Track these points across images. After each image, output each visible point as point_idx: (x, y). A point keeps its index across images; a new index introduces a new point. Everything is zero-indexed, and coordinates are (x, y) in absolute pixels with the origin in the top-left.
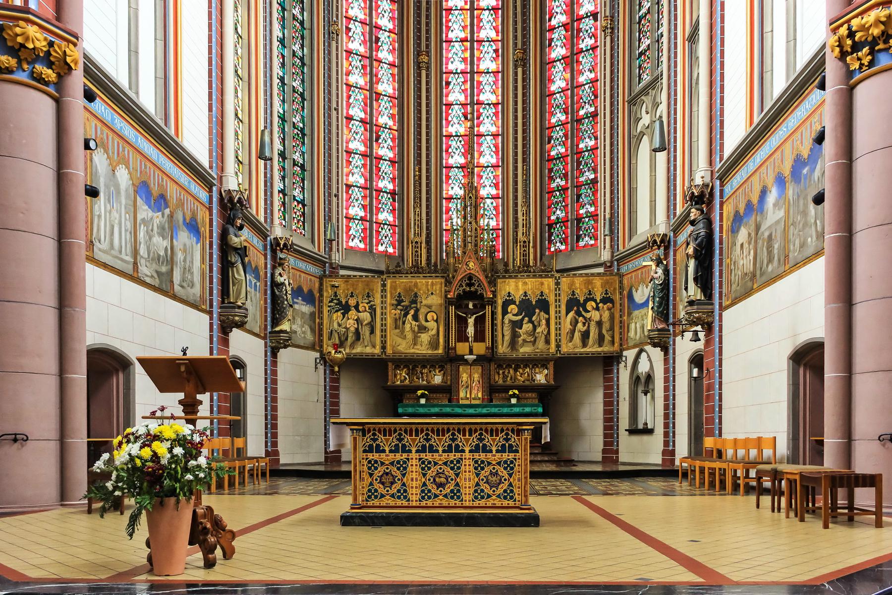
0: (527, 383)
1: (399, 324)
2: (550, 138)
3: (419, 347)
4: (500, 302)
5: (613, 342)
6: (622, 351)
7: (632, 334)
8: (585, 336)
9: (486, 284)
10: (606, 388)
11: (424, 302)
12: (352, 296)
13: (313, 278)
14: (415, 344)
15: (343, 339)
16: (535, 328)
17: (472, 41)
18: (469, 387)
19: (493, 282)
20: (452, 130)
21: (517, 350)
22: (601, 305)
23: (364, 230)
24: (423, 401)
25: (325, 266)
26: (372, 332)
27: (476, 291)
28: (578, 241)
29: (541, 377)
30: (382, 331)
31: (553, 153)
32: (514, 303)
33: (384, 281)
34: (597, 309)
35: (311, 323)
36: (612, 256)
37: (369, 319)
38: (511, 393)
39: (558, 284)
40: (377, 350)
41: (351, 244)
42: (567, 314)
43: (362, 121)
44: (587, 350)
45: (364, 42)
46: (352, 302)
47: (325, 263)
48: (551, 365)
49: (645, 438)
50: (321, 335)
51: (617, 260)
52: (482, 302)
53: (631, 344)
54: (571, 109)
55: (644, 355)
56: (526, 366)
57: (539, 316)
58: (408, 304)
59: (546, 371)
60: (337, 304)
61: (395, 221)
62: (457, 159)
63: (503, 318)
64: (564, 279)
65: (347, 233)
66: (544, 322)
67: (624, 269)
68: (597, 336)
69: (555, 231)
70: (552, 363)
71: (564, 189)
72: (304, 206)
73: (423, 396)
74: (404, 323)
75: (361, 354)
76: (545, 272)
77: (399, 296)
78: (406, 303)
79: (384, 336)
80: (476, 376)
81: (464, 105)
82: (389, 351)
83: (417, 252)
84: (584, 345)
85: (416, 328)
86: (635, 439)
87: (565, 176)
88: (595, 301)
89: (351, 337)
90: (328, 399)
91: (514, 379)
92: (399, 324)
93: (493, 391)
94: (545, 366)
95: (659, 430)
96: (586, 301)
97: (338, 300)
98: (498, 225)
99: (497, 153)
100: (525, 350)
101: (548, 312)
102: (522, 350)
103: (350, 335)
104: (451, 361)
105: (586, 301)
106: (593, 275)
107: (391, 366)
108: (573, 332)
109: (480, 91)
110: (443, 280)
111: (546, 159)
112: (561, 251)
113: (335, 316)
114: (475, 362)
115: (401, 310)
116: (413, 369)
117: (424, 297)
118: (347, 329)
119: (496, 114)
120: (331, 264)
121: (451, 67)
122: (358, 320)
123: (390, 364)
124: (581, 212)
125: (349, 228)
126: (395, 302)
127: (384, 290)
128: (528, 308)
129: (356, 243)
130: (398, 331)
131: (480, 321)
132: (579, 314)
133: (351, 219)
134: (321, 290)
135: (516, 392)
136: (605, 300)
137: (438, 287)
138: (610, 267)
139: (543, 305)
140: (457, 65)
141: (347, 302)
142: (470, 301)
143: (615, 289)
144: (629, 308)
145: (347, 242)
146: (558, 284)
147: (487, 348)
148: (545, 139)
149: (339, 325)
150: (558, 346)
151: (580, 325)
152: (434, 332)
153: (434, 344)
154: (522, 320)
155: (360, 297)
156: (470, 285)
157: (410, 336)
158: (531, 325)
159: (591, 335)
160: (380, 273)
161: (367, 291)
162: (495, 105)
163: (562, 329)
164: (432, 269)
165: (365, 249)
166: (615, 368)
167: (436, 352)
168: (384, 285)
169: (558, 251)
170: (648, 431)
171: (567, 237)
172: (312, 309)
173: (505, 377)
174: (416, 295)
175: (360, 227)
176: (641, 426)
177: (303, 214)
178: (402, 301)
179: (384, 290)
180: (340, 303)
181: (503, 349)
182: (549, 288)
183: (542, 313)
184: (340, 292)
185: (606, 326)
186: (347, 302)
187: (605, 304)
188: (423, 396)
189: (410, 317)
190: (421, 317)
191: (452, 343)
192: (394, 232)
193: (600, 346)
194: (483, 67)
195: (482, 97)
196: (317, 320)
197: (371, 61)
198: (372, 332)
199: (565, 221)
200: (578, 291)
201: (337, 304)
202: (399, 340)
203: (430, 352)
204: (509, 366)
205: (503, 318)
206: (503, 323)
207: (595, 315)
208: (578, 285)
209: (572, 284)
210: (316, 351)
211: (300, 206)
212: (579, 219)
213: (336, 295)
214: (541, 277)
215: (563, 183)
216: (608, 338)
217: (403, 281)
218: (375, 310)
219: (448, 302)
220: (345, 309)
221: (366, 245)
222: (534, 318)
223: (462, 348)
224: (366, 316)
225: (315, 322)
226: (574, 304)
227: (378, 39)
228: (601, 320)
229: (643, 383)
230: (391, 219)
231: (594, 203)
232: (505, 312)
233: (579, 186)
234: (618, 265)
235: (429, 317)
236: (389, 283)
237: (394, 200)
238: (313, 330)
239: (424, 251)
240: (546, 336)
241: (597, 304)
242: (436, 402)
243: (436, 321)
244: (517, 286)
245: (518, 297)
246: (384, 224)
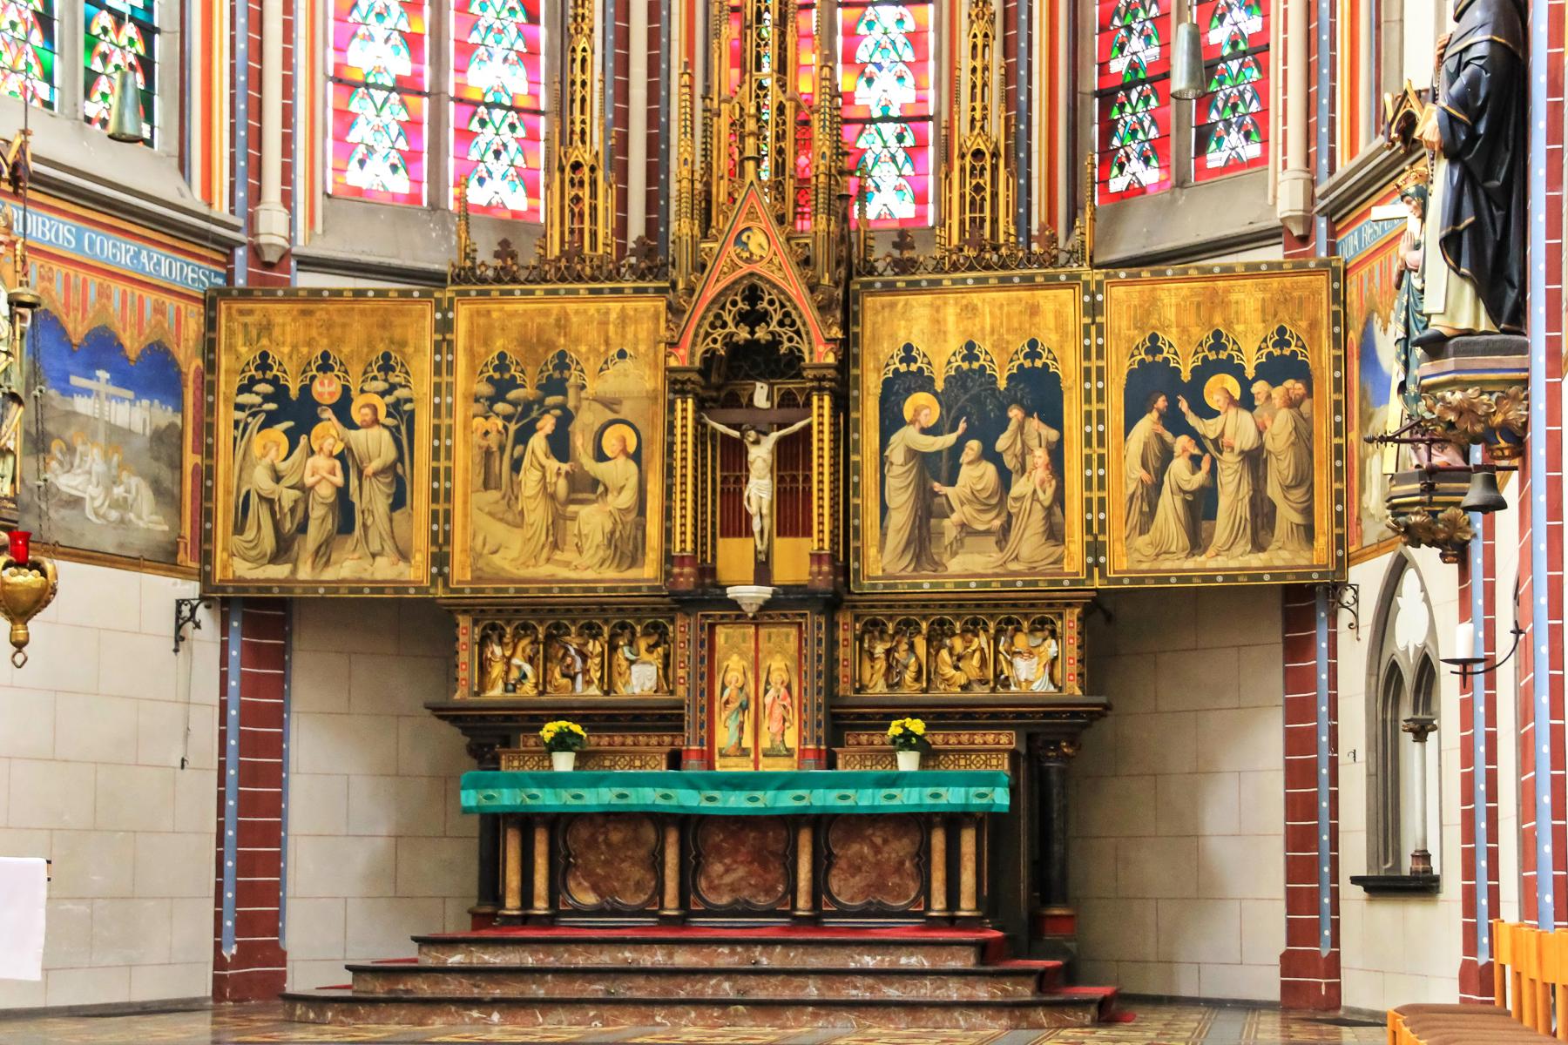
0: (980, 692)
1: (498, 469)
3: (568, 555)
5: (1308, 532)
6: (1343, 564)
8: (1201, 506)
10: (1298, 711)
11: (594, 386)
12: (325, 367)
13: (171, 302)
14: (555, 546)
15: (288, 526)
16: (1005, 478)
21: (937, 565)
22: (1259, 388)
23: (411, 127)
24: (564, 762)
25: (230, 258)
26: (399, 501)
27: (775, 342)
28: (1202, 148)
30: (435, 496)
33: (445, 308)
34: (1247, 402)
35: (166, 475)
36: (1311, 199)
37: (389, 453)
38: (895, 729)
39: (1093, 309)
40: (416, 571)
41: (356, 177)
44: (1207, 561)
46: (326, 389)
47: (231, 245)
48: (1070, 623)
49: (1414, 912)
50: (206, 515)
51: (1329, 213)
53: (1370, 538)
55: (1410, 576)
56: (974, 627)
57: (1024, 434)
58: (534, 398)
59: (1051, 647)
60: (267, 398)
61: (534, 95)
63: (884, 444)
64: (1119, 292)
65: (340, 139)
66: (1040, 456)
67: (1352, 244)
68: (1244, 510)
69: (1125, 118)
70: (1072, 616)
72: (148, 31)
73: (562, 742)
74: (516, 466)
75: (356, 585)
77: (502, 363)
78: (527, 392)
79: (441, 519)
82: (460, 571)
83: (577, 199)
84: (1197, 543)
85: (562, 486)
86: (1389, 913)
88: (1238, 372)
89: (320, 523)
90: (232, 757)
92: (498, 469)
94: (1045, 626)
95: (1452, 885)
96: (1204, 371)
97: (274, 381)
98: (921, 101)
100: (969, 565)
101: (1055, 420)
102: (955, 565)
103: (317, 513)
105: (1204, 371)
106: (1228, 272)
107: (467, 631)
108: (1153, 491)
110: (662, 305)
112: (1142, 190)
113: (258, 441)
115: (508, 418)
116: (550, 638)
117: (591, 366)
118: (305, 490)
120: (256, 251)
122: (345, 458)
123: (464, 621)
125: (345, 119)
126: (485, 389)
127: (444, 345)
128: (977, 404)
129: (380, 175)
130: (493, 495)
131: (792, 454)
132: (1174, 422)
133: (353, 86)
134: (209, 346)
135: (917, 726)
136: (1279, 368)
137: (644, 329)
138: (1304, 240)
139: (1039, 391)
141: (306, 390)
143: (1314, 325)
144: (1363, 397)
145: (339, 171)
146: (1093, 309)
147: (817, 558)
149: (278, 478)
150: (1095, 549)
151: (1179, 468)
152: (627, 498)
153: (625, 547)
154: (957, 449)
155: (356, 370)
156: (753, 318)
157: (537, 514)
158: (990, 469)
159: (1224, 502)
160: (434, 279)
161: (381, 349)
163: (1111, 482)
165: (414, 198)
166: (1322, 632)
167: (632, 574)
168: (445, 326)
169: (1135, 191)
170: (1423, 885)
171: (1165, 136)
172: (163, 415)
173: (892, 670)
174: (562, 362)
175: (395, 113)
176: (1407, 866)
177: (146, 64)
178: (513, 384)
179: (444, 345)
180: (280, 393)
181: (882, 561)
182: (1060, 327)
183: (1034, 424)
184: (280, 354)
185: (1280, 469)
186: (306, 390)
187: (1275, 382)
189: (538, 442)
190: (581, 443)
192: (533, 136)
193: (1258, 546)
196: (191, 460)
198: (399, 501)
200: (1170, 336)
201: (267, 398)
202: (498, 531)
203: (610, 573)
205: (884, 444)
206: (883, 461)
207: (1238, 428)
208: (1170, 314)
209: (1150, 307)
210: (186, 574)
211: (130, 30)
213: (264, 362)
214: (1029, 283)
216: (1287, 515)
217: (518, 313)
218: (410, 418)
220: (296, 414)
221: (416, 182)
222: (1002, 443)
224: (375, 444)
225: (180, 467)
228: (1260, 448)
229: (1406, 692)
230: (516, 82)
232: (891, 421)
234: (1332, 233)
235: (610, 443)
236: (462, 316)
237: (533, 18)
238: (166, 496)
239: (605, 202)
240: (1049, 511)
241: (1246, 385)
243: (637, 457)
244: (937, 322)
245: (941, 360)
246: (490, 106)
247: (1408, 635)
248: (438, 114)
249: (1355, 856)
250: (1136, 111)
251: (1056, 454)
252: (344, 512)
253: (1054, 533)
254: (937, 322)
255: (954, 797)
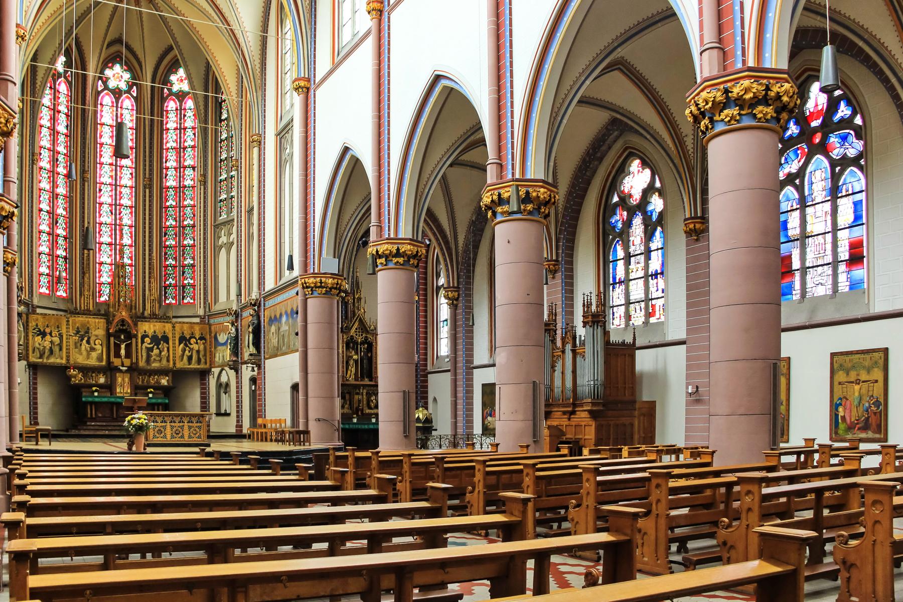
2: (166, 234)
4: (140, 336)
7: (217, 359)
8: (190, 358)
9: (132, 325)
17: (116, 166)
18: (122, 386)
19: (136, 325)
20: (103, 220)
29: (164, 382)
31: (167, 243)
32: (147, 336)
34: (197, 343)
39: (174, 327)
42: (180, 344)
43: (48, 212)
44: (191, 366)
45: (49, 162)
48: (170, 374)
49: (226, 418)
52: (129, 336)
54: (180, 219)
57: (163, 345)
62: (106, 239)
71: (175, 267)
76: (165, 318)
80: (127, 380)
81: (111, 205)
84: (190, 363)
87: (175, 258)
91: (148, 381)
93: (137, 389)
94: (167, 375)
96: (191, 338)
99: (131, 237)
100: (155, 365)
101: (168, 343)
104: (110, 370)
105: (191, 338)
109: (121, 198)
111: (163, 247)
114: (126, 371)
119: (131, 213)
121: (103, 180)
124: (186, 282)
132: (186, 345)
136: (201, 338)
139: (166, 339)
140: (106, 179)
142: (121, 334)
146: (174, 327)
148: (163, 233)
150: (174, 364)
151: (187, 352)
156: (123, 325)
162: (131, 207)
164: (97, 314)
169: (170, 304)
185: (202, 353)
188: (96, 391)
191: (113, 359)
194: (123, 182)
195: (122, 202)
197: (53, 173)
199: (175, 286)
200: (185, 332)
204: (145, 374)
207: (196, 347)
212: (184, 286)
215: (174, 263)
216: (203, 360)
217: (81, 319)
219: (109, 335)
223: (116, 362)
226: (182, 339)
227: (57, 160)
229: (223, 388)
231: (193, 278)
232: (143, 342)
233: (184, 266)
236: (71, 320)
242: (103, 395)
244: (150, 328)
245: (150, 333)
247: (224, 379)
248: (55, 281)
249: (213, 409)
250: (170, 290)
251: (168, 349)
252: (51, 351)
253: (168, 361)
254: (150, 328)
255: (160, 401)
